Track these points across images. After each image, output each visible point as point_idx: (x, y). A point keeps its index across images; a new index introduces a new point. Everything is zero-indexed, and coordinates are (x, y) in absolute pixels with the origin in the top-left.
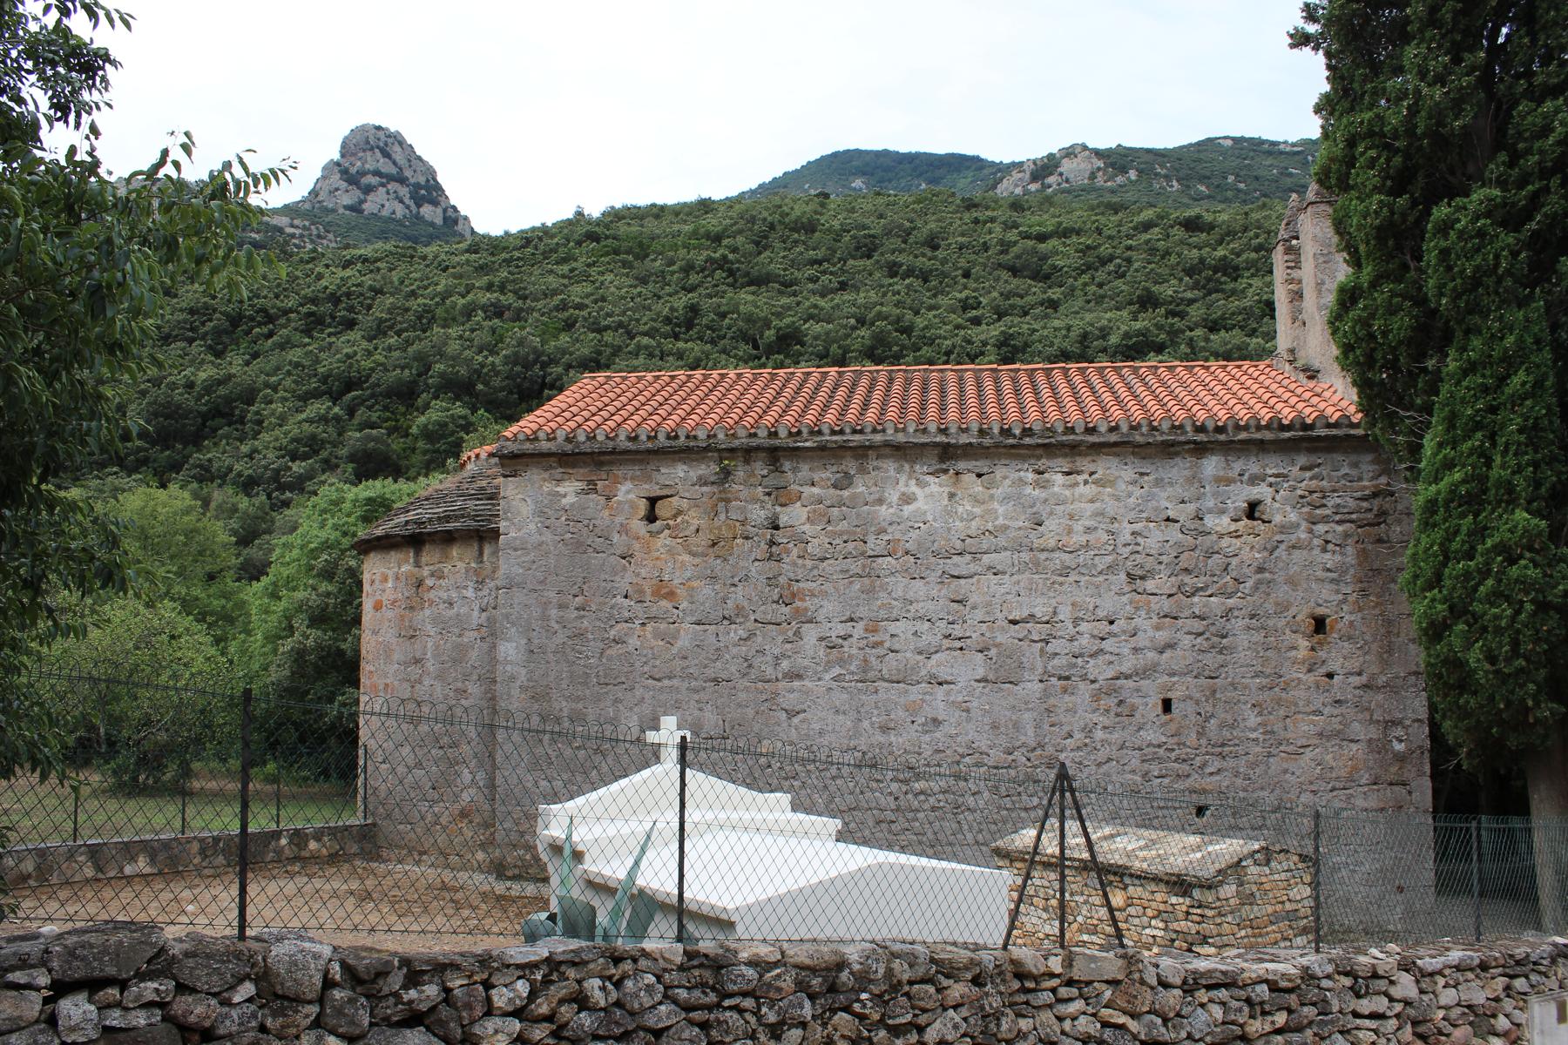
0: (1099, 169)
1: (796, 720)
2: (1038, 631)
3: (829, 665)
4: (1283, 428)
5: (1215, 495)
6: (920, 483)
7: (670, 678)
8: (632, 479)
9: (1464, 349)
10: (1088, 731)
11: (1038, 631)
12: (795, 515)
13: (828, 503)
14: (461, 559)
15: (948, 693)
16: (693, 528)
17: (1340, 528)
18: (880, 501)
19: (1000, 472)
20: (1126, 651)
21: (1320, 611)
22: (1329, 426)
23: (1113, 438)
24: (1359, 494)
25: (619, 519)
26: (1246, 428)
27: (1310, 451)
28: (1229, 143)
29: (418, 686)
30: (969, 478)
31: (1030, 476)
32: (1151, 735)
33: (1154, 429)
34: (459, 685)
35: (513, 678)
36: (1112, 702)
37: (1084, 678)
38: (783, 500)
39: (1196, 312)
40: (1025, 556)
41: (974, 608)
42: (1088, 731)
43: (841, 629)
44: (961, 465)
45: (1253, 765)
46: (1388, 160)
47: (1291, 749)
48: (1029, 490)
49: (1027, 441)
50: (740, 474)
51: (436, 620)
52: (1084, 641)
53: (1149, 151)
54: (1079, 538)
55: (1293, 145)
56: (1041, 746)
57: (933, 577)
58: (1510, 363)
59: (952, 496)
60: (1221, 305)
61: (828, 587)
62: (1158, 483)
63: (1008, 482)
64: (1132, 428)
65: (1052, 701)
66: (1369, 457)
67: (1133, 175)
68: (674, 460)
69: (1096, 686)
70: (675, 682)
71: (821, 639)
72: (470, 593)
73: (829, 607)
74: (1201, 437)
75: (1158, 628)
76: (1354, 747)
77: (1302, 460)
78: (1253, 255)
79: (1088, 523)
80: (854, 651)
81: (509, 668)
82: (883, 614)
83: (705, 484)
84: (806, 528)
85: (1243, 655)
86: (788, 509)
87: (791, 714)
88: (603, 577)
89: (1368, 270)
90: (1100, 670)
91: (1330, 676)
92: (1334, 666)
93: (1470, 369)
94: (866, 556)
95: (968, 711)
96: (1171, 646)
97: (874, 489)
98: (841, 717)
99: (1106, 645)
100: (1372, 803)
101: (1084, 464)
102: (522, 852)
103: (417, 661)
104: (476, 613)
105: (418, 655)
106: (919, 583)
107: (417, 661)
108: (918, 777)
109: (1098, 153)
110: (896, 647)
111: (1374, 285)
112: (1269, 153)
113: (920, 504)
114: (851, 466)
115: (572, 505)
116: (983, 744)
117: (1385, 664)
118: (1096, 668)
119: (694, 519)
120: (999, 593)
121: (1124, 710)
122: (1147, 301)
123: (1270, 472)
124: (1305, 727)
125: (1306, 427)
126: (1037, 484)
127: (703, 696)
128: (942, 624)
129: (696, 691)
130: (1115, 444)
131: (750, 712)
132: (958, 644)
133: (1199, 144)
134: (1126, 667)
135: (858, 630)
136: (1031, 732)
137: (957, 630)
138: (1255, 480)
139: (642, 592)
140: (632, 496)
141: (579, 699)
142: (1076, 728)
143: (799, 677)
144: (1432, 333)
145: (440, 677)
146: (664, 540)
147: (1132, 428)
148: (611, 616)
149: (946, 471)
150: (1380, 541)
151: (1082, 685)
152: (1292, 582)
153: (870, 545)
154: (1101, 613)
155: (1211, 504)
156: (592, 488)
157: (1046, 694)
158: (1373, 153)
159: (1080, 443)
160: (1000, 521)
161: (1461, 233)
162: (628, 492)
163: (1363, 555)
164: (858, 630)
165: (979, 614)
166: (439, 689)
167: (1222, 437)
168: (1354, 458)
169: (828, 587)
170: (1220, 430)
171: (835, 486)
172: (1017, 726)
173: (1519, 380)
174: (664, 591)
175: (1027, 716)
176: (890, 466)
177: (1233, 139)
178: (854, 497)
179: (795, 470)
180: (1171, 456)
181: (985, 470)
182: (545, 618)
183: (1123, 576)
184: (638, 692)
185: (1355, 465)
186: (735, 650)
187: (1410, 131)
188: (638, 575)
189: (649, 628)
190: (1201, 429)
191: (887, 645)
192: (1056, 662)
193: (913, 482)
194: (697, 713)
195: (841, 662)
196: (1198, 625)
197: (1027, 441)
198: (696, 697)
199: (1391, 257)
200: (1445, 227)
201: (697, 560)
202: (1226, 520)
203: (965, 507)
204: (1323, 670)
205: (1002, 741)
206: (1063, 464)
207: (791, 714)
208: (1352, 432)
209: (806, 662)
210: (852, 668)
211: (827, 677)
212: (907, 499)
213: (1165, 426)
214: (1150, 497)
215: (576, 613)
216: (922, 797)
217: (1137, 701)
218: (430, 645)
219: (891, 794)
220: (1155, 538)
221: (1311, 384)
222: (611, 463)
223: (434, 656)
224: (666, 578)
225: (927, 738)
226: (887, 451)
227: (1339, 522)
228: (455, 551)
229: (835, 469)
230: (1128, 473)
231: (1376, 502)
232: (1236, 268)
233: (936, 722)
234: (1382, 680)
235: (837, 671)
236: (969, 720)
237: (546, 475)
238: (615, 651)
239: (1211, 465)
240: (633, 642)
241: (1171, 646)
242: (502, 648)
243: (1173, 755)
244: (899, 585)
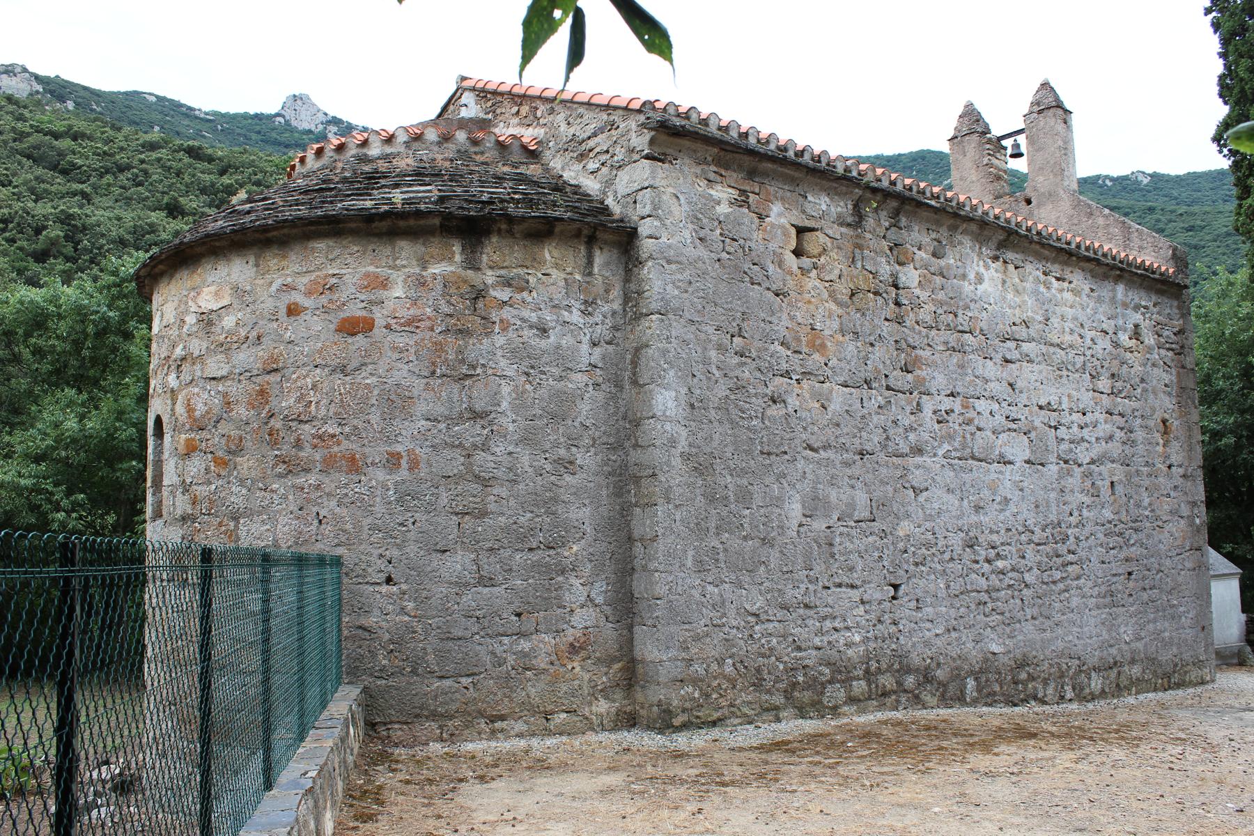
1: (921, 498)
6: (987, 267)
7: (824, 448)
8: (782, 199)
12: (910, 276)
13: (932, 270)
14: (556, 266)
16: (837, 272)
19: (1029, 267)
20: (1093, 440)
21: (1167, 416)
24: (1175, 330)
25: (773, 246)
28: (154, 99)
29: (480, 457)
30: (1011, 267)
32: (1108, 514)
34: (562, 452)
35: (673, 442)
36: (1088, 483)
38: (902, 258)
40: (1044, 348)
41: (1021, 392)
43: (947, 403)
44: (1010, 255)
45: (1148, 536)
47: (1160, 523)
50: (870, 222)
51: (514, 354)
53: (85, 88)
54: (1067, 338)
55: (207, 114)
56: (1059, 524)
57: (998, 358)
59: (1004, 282)
63: (1031, 278)
66: (1175, 303)
68: (823, 189)
69: (1082, 469)
70: (830, 454)
72: (576, 317)
73: (939, 381)
77: (1154, 298)
81: (668, 427)
82: (971, 391)
83: (841, 224)
84: (917, 292)
86: (906, 269)
87: (917, 491)
88: (763, 315)
91: (1169, 467)
92: (1174, 459)
94: (960, 329)
95: (1021, 490)
96: (1111, 437)
97: (959, 264)
98: (951, 496)
102: (690, 689)
103: (476, 415)
104: (585, 347)
105: (478, 407)
107: (476, 415)
110: (981, 426)
112: (187, 116)
114: (944, 233)
115: (727, 216)
119: (835, 263)
123: (1143, 303)
124: (1166, 506)
127: (856, 470)
128: (1004, 404)
129: (847, 464)
133: (126, 93)
138: (1137, 308)
139: (798, 340)
140: (783, 221)
141: (744, 472)
142: (1074, 506)
145: (525, 440)
146: (812, 282)
148: (771, 367)
152: (1154, 393)
153: (960, 319)
156: (742, 201)
157: (1060, 478)
160: (1030, 314)
162: (780, 215)
165: (1023, 399)
166: (525, 460)
171: (934, 255)
174: (818, 342)
175: (1053, 495)
176: (967, 242)
177: (157, 97)
178: (949, 267)
179: (908, 228)
181: (1021, 264)
182: (706, 362)
184: (800, 464)
186: (875, 418)
188: (792, 318)
189: (805, 383)
191: (976, 422)
193: (981, 263)
194: (848, 490)
195: (950, 437)
198: (849, 471)
201: (840, 311)
206: (1056, 269)
207: (917, 491)
215: (737, 359)
216: (1001, 576)
218: (506, 389)
219: (983, 575)
222: (765, 174)
223: (516, 409)
224: (818, 326)
225: (1001, 517)
226: (974, 227)
227: (1168, 349)
228: (548, 253)
229: (934, 235)
233: (1006, 501)
235: (946, 447)
237: (698, 170)
238: (775, 411)
240: (793, 402)
242: (660, 398)
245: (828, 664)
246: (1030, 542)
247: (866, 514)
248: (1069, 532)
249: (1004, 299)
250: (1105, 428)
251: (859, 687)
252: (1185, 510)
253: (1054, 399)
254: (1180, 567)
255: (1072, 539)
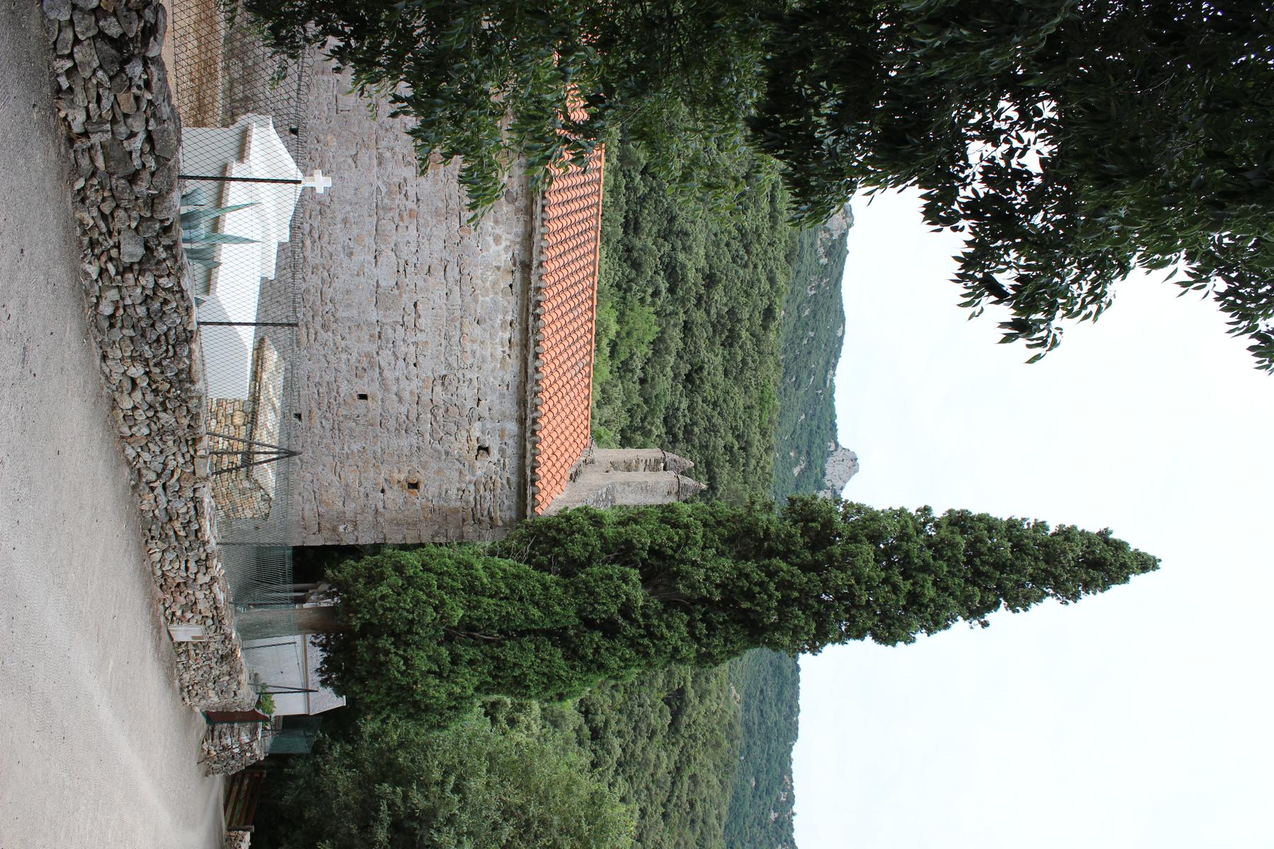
0: (831, 235)
1: (350, 161)
2: (410, 320)
3: (388, 185)
4: (533, 469)
5: (494, 429)
6: (507, 248)
9: (557, 584)
10: (346, 350)
11: (410, 320)
15: (369, 263)
17: (471, 499)
18: (496, 222)
19: (513, 299)
21: (422, 486)
22: (533, 494)
23: (530, 371)
26: (534, 447)
27: (519, 483)
31: (509, 318)
32: (344, 388)
33: (536, 394)
36: (365, 365)
37: (380, 347)
39: (699, 316)
40: (458, 313)
42: (346, 350)
43: (411, 194)
44: (518, 275)
45: (327, 447)
46: (671, 547)
47: (338, 468)
48: (500, 317)
49: (531, 318)
52: (404, 349)
54: (468, 347)
57: (445, 254)
58: (546, 609)
59: (498, 268)
60: (702, 335)
61: (440, 185)
62: (502, 395)
63: (506, 304)
64: (537, 381)
65: (365, 328)
66: (514, 516)
67: (824, 261)
71: (405, 180)
74: (529, 422)
75: (411, 393)
76: (341, 504)
77: (514, 479)
78: (739, 358)
79: (478, 353)
80: (397, 202)
82: (421, 221)
85: (395, 443)
87: (355, 158)
89: (609, 532)
90: (385, 357)
91: (383, 491)
92: (389, 493)
93: (545, 588)
96: (400, 400)
99: (401, 362)
100: (307, 514)
101: (516, 351)
106: (442, 245)
108: (313, 242)
109: (844, 235)
111: (601, 536)
113: (493, 248)
114: (521, 203)
116: (336, 284)
117: (391, 522)
118: (386, 356)
120: (434, 296)
121: (359, 372)
122: (710, 280)
124: (351, 477)
125: (533, 482)
126: (504, 322)
130: (526, 372)
131: (355, 130)
132: (401, 270)
134: (387, 373)
135: (411, 205)
136: (345, 314)
137: (410, 269)
138: (502, 451)
142: (348, 342)
143: (380, 164)
144: (570, 568)
147: (537, 381)
149: (514, 264)
150: (464, 520)
151: (375, 346)
152: (439, 471)
154: (421, 359)
155: (488, 426)
157: (369, 324)
158: (676, 538)
159: (528, 351)
160: (481, 298)
161: (619, 586)
163: (456, 511)
164: (411, 205)
165: (420, 284)
167: (528, 434)
168: (514, 507)
169: (440, 185)
170: (534, 433)
172: (349, 306)
173: (535, 613)
175: (355, 312)
176: (519, 228)
180: (518, 404)
183: (444, 373)
185: (509, 508)
187: (683, 561)
190: (534, 421)
192: (390, 331)
195: (390, 193)
196: (413, 416)
197: (531, 318)
199: (615, 545)
200: (625, 579)
202: (478, 434)
203: (490, 276)
204: (386, 488)
205: (338, 297)
206: (516, 338)
207: (355, 158)
208: (529, 508)
209: (389, 169)
210: (386, 200)
211: (380, 183)
212: (497, 240)
213: (537, 401)
214: (493, 390)
217: (366, 380)
220: (468, 393)
221: (567, 477)
225: (340, 248)
227: (475, 499)
230: (509, 377)
231: (487, 519)
232: (731, 345)
234: (381, 519)
235: (384, 190)
236: (352, 275)
239: (512, 427)
241: (400, 400)
243: (332, 400)
244: (440, 232)
245: (255, 64)
246: (323, 281)
247: (341, 107)
248: (330, 334)
249: (487, 267)
250: (408, 388)
251: (239, 91)
252: (350, 508)
253: (422, 322)
254: (305, 494)
255: (325, 336)
